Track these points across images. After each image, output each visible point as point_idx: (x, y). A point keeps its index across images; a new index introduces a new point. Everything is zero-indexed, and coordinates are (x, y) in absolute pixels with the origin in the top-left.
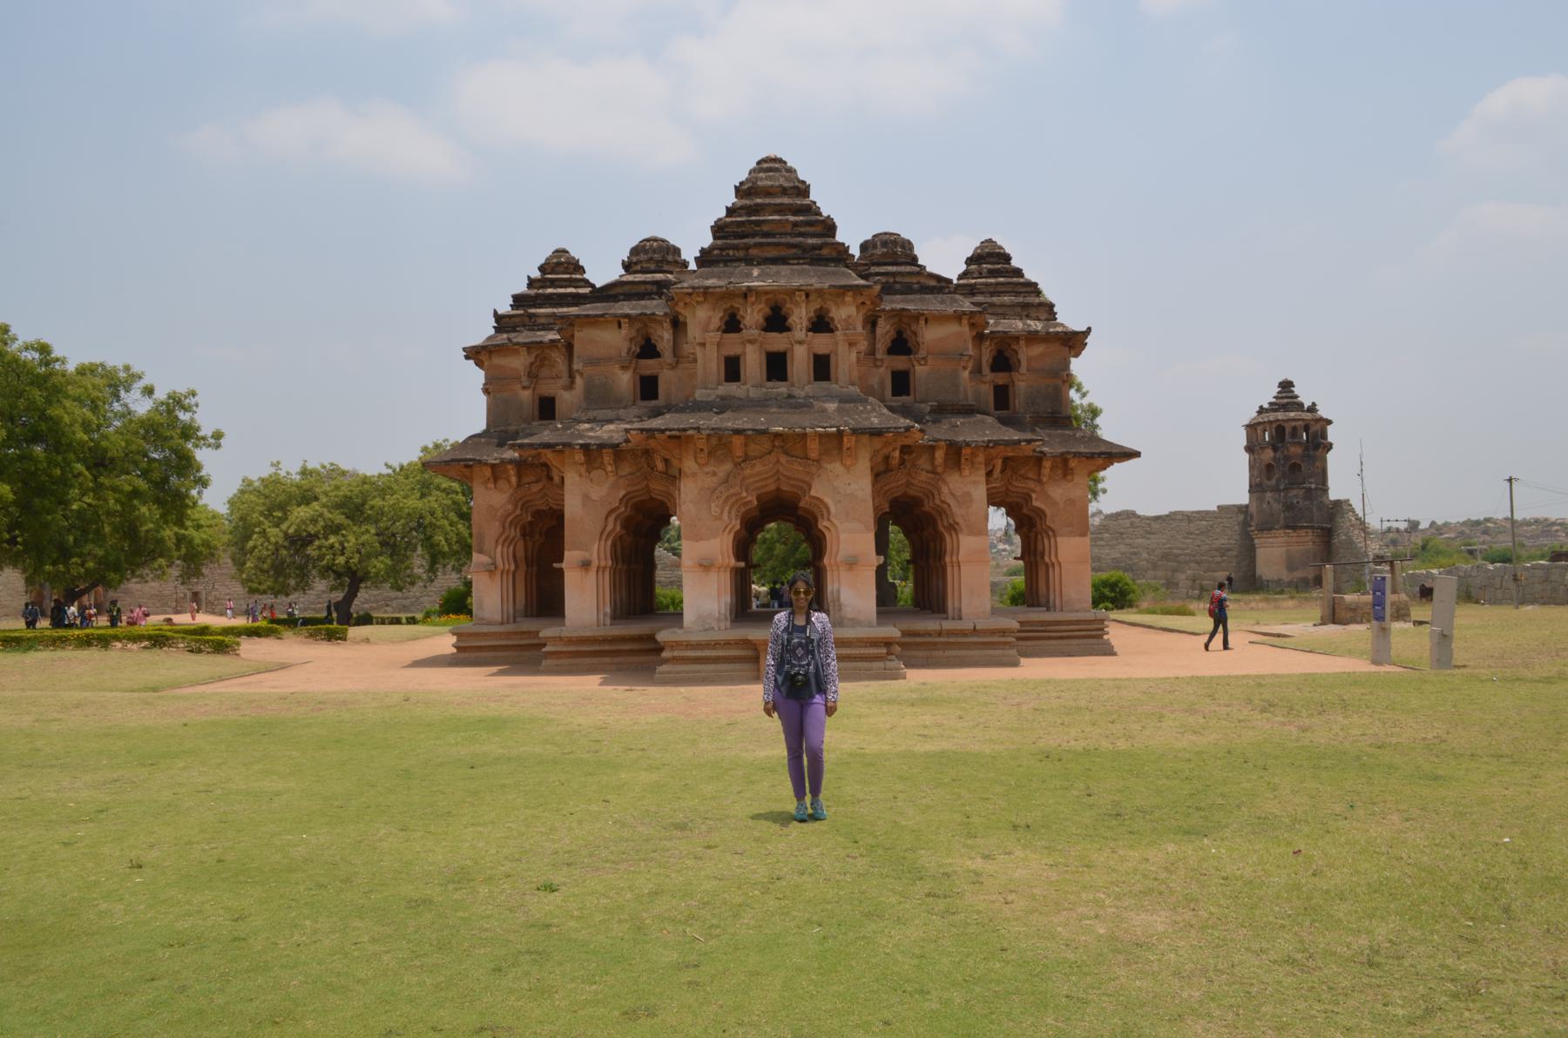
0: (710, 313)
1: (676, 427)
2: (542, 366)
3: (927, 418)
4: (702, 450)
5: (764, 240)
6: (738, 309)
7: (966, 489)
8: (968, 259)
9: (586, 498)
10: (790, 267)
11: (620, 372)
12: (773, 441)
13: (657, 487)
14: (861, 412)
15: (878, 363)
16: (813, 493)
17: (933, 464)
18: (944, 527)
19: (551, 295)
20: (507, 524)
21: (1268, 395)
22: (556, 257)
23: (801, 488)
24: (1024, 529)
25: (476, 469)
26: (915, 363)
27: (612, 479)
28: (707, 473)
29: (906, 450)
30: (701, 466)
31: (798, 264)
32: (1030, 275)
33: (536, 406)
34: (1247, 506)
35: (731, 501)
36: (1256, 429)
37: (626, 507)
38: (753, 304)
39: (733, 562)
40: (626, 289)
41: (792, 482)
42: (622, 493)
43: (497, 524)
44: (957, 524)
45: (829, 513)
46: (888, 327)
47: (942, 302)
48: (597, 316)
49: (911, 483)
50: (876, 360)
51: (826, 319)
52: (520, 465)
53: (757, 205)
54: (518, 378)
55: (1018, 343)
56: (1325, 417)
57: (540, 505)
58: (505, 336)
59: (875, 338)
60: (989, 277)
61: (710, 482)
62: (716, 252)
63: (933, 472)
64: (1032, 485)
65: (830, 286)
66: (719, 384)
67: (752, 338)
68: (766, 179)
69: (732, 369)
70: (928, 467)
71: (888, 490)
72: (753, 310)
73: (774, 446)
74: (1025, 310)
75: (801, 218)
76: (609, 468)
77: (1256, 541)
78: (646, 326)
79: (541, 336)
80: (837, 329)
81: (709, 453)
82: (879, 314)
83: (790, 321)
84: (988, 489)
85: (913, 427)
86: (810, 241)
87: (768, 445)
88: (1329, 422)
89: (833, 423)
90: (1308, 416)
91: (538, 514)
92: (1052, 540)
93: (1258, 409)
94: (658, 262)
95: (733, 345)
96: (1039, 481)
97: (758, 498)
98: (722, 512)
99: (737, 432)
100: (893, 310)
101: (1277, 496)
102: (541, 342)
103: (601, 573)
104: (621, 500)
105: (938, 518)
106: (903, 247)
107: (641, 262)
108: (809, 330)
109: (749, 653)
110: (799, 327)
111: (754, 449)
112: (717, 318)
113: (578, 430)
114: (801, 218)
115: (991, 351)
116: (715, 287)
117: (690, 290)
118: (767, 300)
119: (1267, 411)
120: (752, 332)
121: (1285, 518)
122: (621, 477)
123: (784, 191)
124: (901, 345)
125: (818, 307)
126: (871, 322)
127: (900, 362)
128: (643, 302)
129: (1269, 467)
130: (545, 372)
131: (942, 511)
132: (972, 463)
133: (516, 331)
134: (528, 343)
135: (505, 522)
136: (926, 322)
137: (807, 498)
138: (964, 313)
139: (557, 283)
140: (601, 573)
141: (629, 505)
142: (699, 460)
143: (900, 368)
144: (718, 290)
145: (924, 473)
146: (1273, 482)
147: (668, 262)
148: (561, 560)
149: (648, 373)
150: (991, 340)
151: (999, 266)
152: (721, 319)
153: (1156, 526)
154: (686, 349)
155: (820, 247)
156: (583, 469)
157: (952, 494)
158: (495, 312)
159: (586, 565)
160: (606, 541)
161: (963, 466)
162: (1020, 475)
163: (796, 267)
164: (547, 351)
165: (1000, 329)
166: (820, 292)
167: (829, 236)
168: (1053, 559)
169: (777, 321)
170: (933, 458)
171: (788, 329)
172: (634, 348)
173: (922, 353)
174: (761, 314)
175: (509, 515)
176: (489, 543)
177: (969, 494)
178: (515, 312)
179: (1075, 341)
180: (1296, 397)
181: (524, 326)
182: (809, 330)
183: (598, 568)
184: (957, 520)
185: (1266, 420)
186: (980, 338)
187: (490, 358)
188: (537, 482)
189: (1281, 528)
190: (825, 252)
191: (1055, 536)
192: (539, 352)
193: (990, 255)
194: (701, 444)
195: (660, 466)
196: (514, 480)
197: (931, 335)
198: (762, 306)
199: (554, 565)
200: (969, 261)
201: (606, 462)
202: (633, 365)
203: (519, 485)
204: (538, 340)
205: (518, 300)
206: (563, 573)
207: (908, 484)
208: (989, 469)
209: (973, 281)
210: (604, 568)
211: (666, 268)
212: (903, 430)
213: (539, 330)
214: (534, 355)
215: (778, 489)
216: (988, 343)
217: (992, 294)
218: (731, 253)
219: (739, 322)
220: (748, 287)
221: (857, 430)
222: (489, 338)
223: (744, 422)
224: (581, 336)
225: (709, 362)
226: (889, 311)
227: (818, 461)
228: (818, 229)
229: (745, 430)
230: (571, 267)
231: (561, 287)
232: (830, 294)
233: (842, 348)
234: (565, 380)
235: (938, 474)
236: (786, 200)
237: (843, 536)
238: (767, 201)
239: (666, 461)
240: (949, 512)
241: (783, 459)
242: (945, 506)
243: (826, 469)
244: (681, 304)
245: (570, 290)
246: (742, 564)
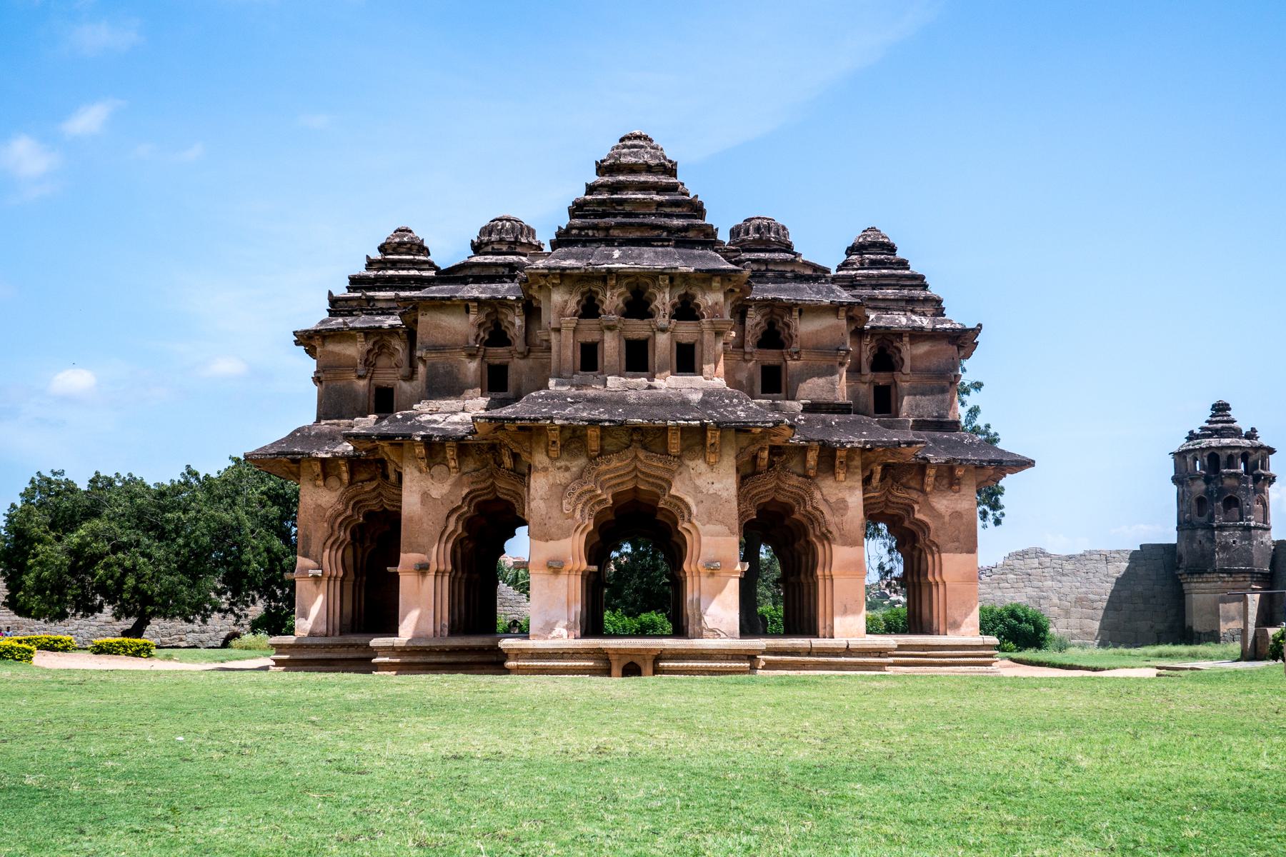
0: (566, 297)
1: (527, 416)
2: (378, 355)
3: (800, 417)
4: (554, 442)
5: (624, 220)
6: (597, 293)
7: (840, 495)
8: (848, 248)
9: (425, 496)
10: (653, 249)
11: (467, 360)
12: (631, 435)
13: (504, 486)
14: (727, 405)
15: (747, 357)
16: (673, 492)
17: (805, 467)
18: (816, 536)
19: (391, 277)
20: (337, 525)
21: (1200, 418)
22: (398, 236)
23: (661, 487)
24: (907, 547)
25: (305, 465)
26: (788, 358)
27: (454, 476)
28: (558, 469)
29: (776, 451)
30: (552, 459)
31: (662, 246)
32: (915, 268)
33: (373, 398)
34: (1175, 545)
35: (584, 500)
36: (1185, 457)
37: (469, 507)
38: (613, 288)
39: (584, 565)
40: (475, 271)
41: (651, 480)
42: (465, 491)
43: (326, 525)
44: (831, 533)
45: (690, 513)
46: (759, 318)
47: (819, 292)
48: (443, 298)
49: (780, 488)
50: (745, 353)
51: (692, 306)
52: (354, 462)
53: (619, 182)
54: (354, 367)
55: (902, 341)
56: (1266, 444)
57: (374, 505)
58: (340, 320)
59: (744, 330)
60: (872, 269)
61: (562, 477)
62: (574, 232)
63: (806, 476)
64: (914, 495)
65: (696, 270)
66: (574, 373)
67: (611, 323)
68: (629, 155)
69: (589, 358)
70: (799, 470)
71: (755, 495)
72: (612, 295)
73: (632, 440)
74: (910, 304)
75: (667, 197)
76: (452, 464)
77: (1185, 586)
78: (496, 311)
79: (377, 321)
80: (703, 317)
81: (562, 446)
82: (750, 304)
83: (652, 306)
84: (864, 500)
85: (782, 422)
86: (677, 222)
87: (625, 440)
88: (1271, 451)
89: (696, 415)
90: (1247, 443)
91: (369, 515)
92: (936, 556)
93: (1188, 435)
94: (510, 243)
95: (590, 331)
96: (923, 491)
97: (614, 496)
98: (574, 511)
99: (593, 422)
100: (764, 300)
101: (1209, 535)
102: (380, 327)
103: (439, 578)
104: (464, 499)
105: (810, 527)
106: (777, 233)
107: (493, 242)
108: (672, 317)
109: (601, 665)
110: (662, 313)
111: (610, 443)
112: (572, 305)
113: (419, 421)
114: (667, 197)
115: (871, 348)
116: (573, 268)
117: (546, 271)
118: (627, 284)
119: (1197, 437)
120: (611, 317)
122: (467, 473)
123: (649, 169)
124: (773, 338)
125: (683, 292)
126: (740, 312)
127: (771, 357)
128: (493, 286)
129: (1200, 501)
130: (383, 361)
131: (814, 518)
132: (848, 467)
133: (354, 315)
134: (367, 328)
135: (334, 523)
136: (800, 312)
137: (666, 497)
138: (841, 304)
139: (399, 265)
140: (439, 578)
141: (473, 504)
142: (551, 454)
143: (771, 363)
144: (577, 271)
145: (795, 477)
147: (522, 244)
148: (396, 564)
149: (497, 362)
150: (872, 336)
151: (882, 257)
152: (578, 303)
153: (1068, 567)
154: (540, 335)
155: (686, 229)
156: (423, 465)
157: (826, 500)
158: (330, 293)
159: (423, 569)
160: (446, 543)
161: (838, 470)
162: (902, 484)
163: (660, 249)
164: (386, 337)
165: (881, 324)
166: (685, 276)
167: (695, 217)
168: (938, 578)
169: (638, 306)
170: (804, 461)
171: (650, 315)
172: (482, 334)
173: (795, 347)
174: (621, 299)
175: (340, 515)
176: (315, 547)
177: (843, 501)
178: (352, 295)
179: (963, 340)
180: (1233, 421)
181: (361, 310)
182: (672, 317)
183: (437, 572)
184: (831, 529)
185: (1197, 447)
186: (858, 334)
187: (324, 345)
188: (371, 480)
189: (1215, 571)
190: (691, 235)
191: (939, 552)
192: (378, 338)
193: (874, 245)
194: (554, 435)
195: (508, 462)
196: (345, 477)
197: (806, 328)
198: (623, 289)
199: (388, 568)
200: (850, 251)
201: (448, 456)
202: (481, 353)
203: (351, 483)
204: (377, 325)
205: (356, 283)
206: (399, 576)
207: (778, 489)
208: (868, 473)
209: (854, 273)
210: (443, 573)
211: (519, 250)
212: (771, 424)
213: (378, 314)
214: (371, 343)
215: (636, 489)
216: (868, 340)
217: (874, 287)
218: (590, 233)
219: (598, 307)
220: (608, 269)
221: (722, 423)
222: (323, 322)
223: (600, 413)
224: (426, 321)
225: (564, 348)
226: (759, 300)
227: (679, 457)
228: (685, 210)
229: (601, 421)
230: (416, 247)
231: (403, 269)
232: (697, 279)
233: (708, 337)
234: (404, 370)
235: (810, 477)
236: (651, 179)
237: (704, 540)
238: (631, 178)
239: (516, 457)
240: (821, 520)
241: (642, 455)
242: (817, 513)
243: (688, 466)
244: (535, 287)
245: (413, 272)
246: (595, 568)
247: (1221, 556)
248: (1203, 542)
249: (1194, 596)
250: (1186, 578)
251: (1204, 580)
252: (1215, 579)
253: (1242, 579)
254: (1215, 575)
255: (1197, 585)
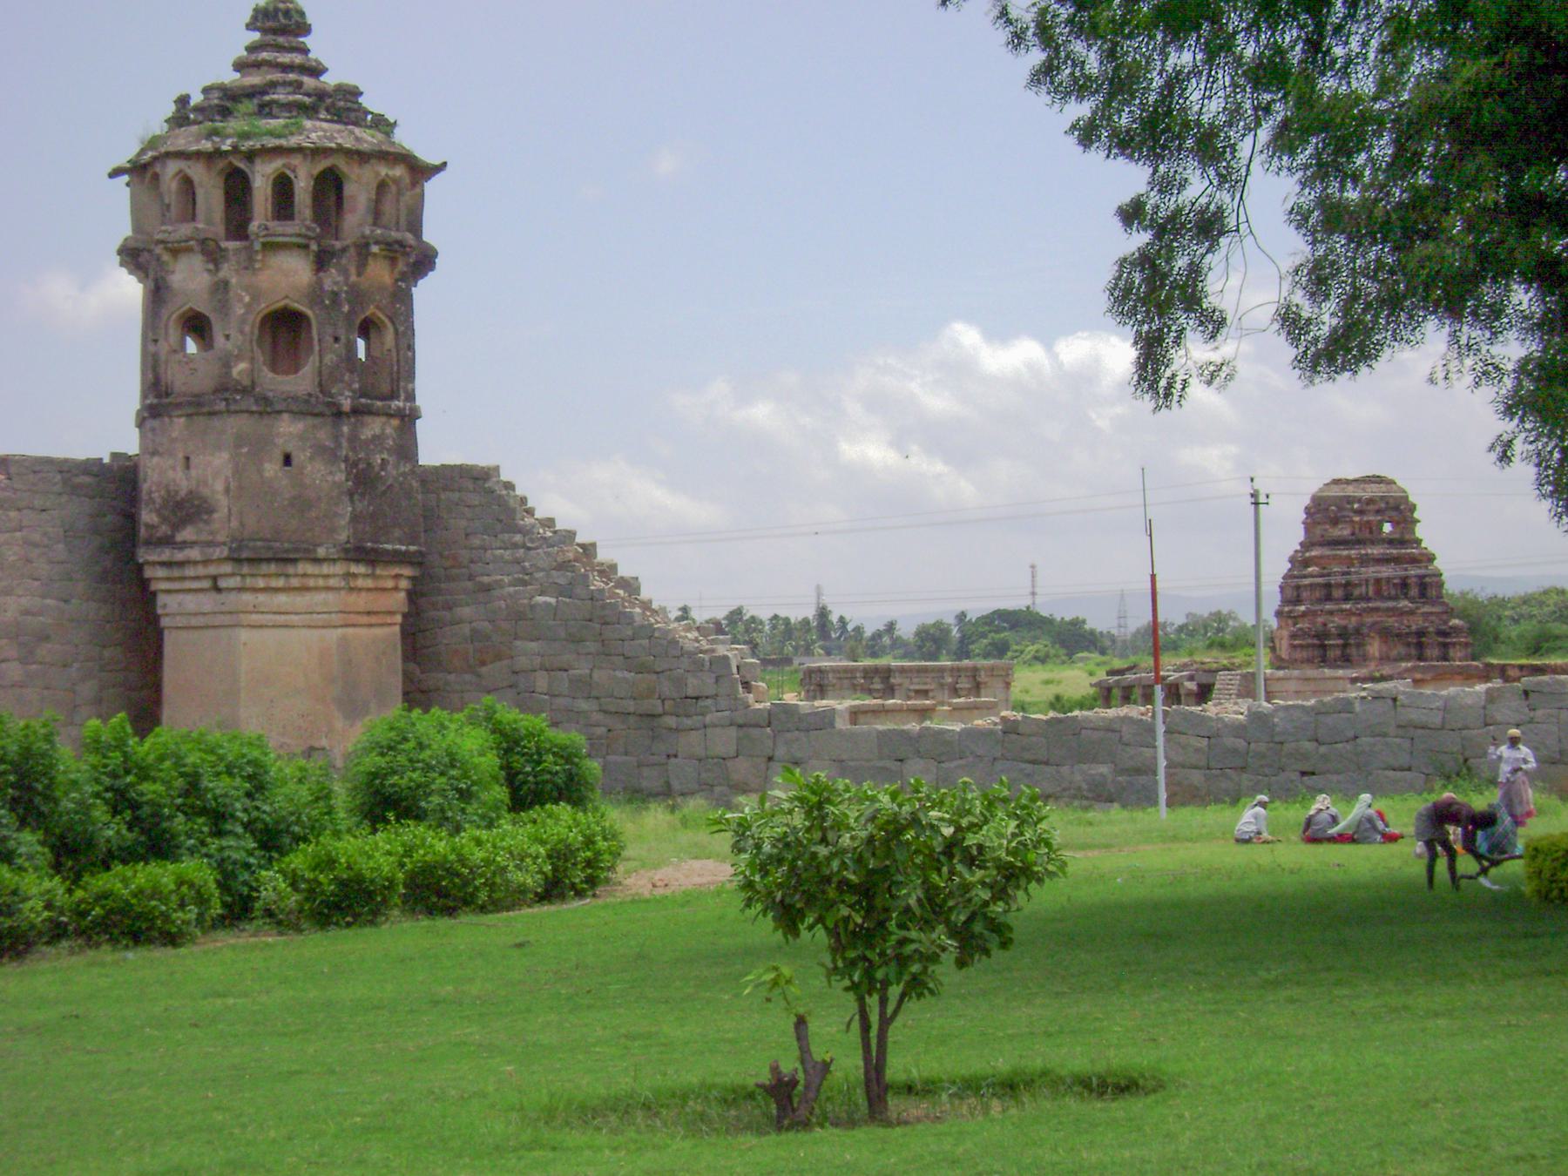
121: (355, 518)
146: (302, 382)
247: (360, 506)
248: (299, 457)
249: (244, 635)
250: (215, 578)
251: (295, 582)
252: (332, 582)
253: (390, 584)
254: (339, 568)
255: (262, 597)
